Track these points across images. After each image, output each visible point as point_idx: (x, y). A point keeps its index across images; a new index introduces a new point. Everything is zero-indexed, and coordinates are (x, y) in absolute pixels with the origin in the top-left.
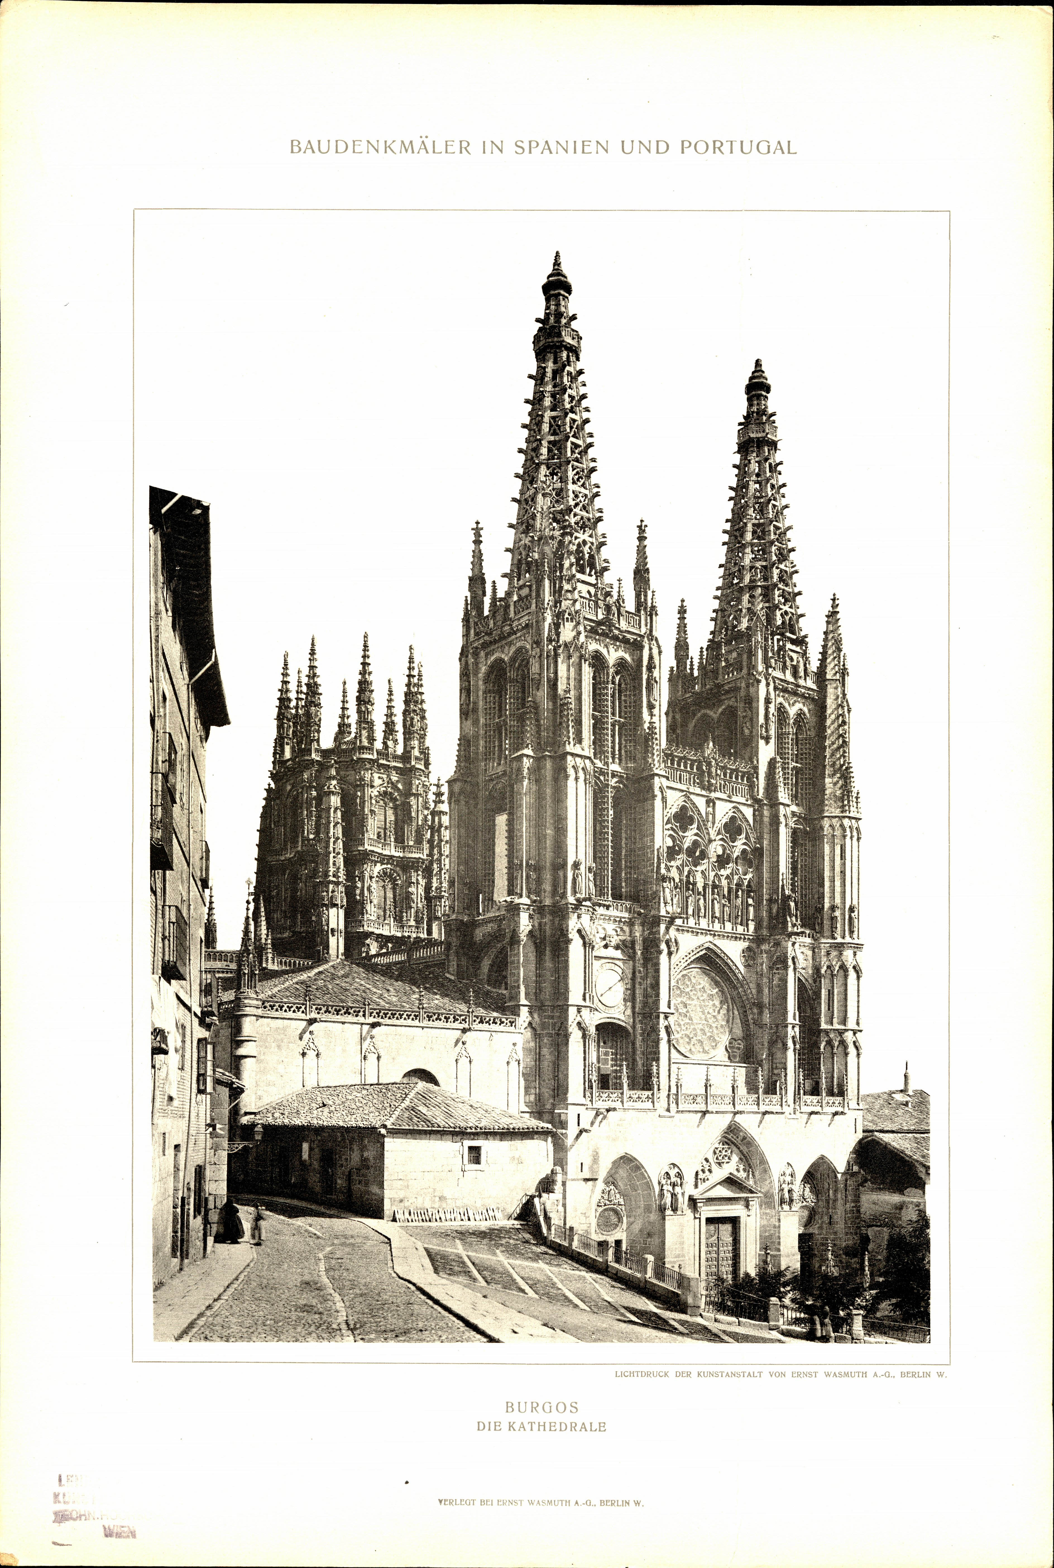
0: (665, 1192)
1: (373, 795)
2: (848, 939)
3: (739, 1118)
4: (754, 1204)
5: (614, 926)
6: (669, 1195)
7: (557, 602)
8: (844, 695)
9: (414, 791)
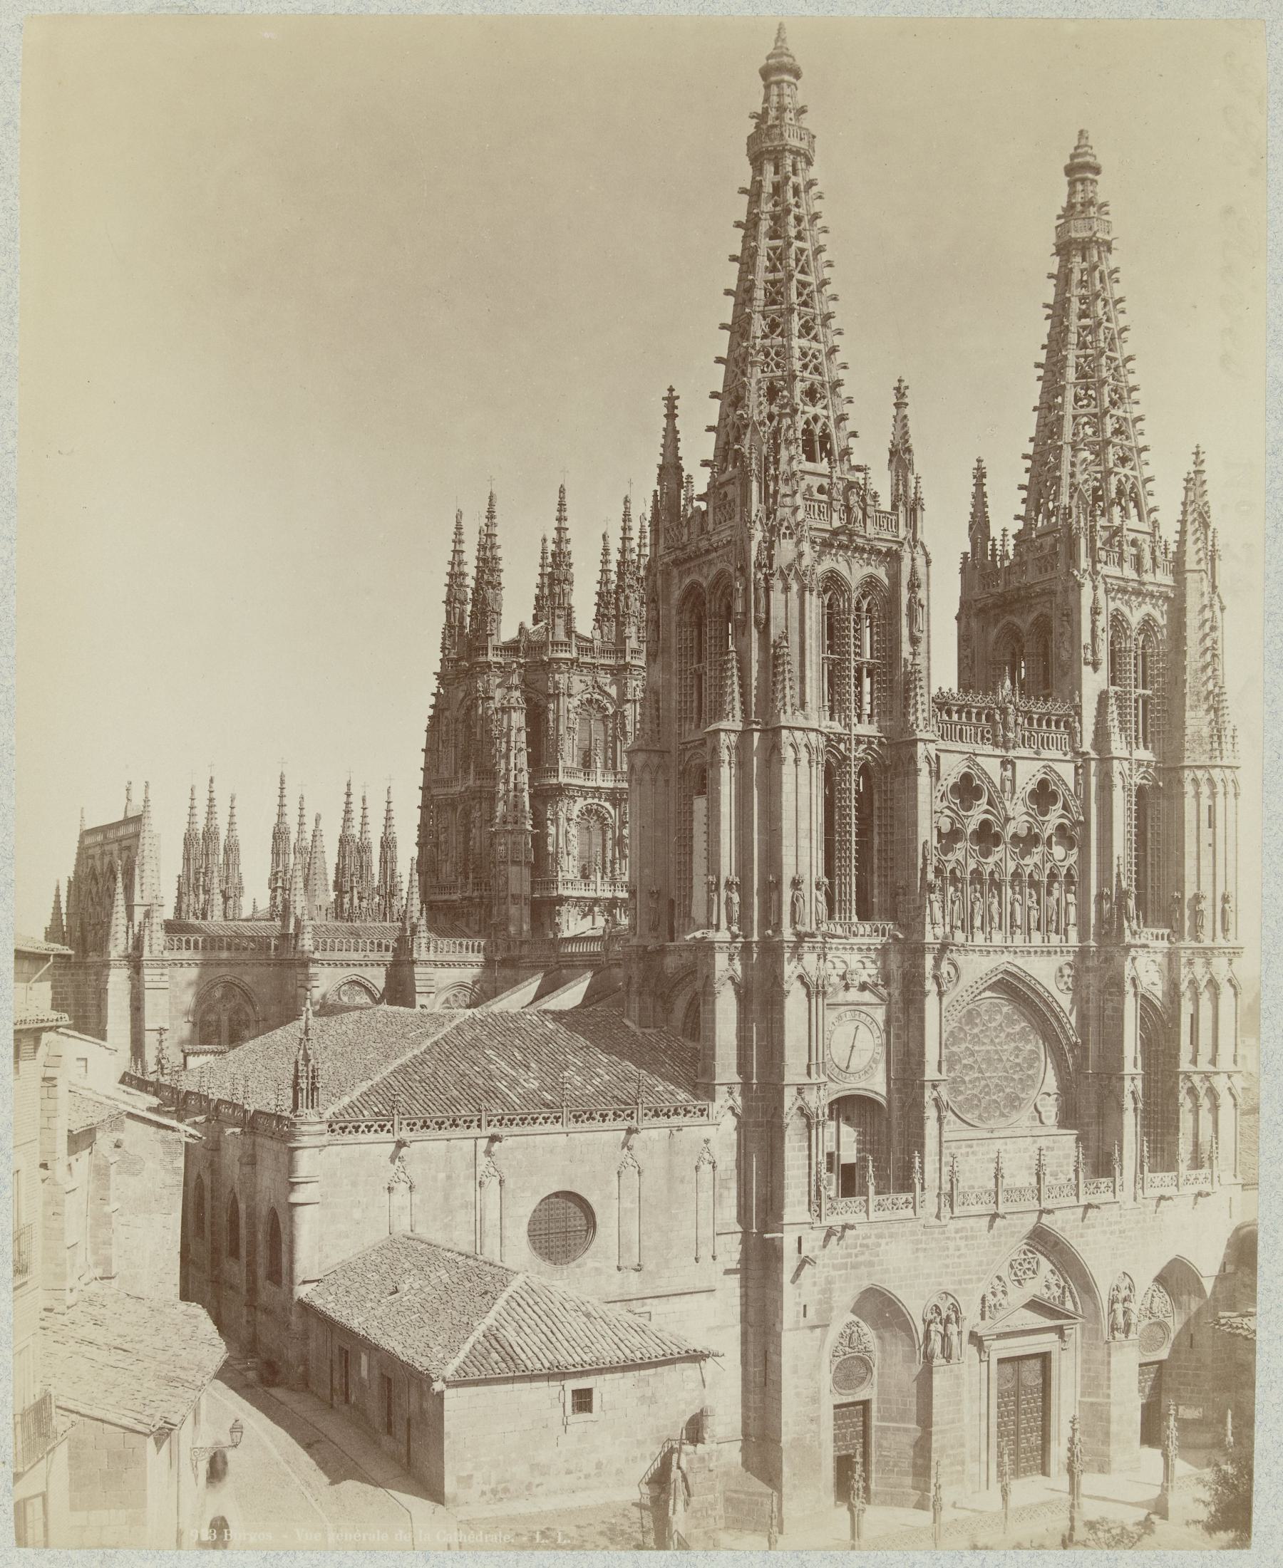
0: (933, 1334)
2: (1220, 941)
3: (1046, 1219)
4: (1075, 1333)
5: (858, 957)
6: (939, 1338)
7: (770, 512)
8: (1214, 587)
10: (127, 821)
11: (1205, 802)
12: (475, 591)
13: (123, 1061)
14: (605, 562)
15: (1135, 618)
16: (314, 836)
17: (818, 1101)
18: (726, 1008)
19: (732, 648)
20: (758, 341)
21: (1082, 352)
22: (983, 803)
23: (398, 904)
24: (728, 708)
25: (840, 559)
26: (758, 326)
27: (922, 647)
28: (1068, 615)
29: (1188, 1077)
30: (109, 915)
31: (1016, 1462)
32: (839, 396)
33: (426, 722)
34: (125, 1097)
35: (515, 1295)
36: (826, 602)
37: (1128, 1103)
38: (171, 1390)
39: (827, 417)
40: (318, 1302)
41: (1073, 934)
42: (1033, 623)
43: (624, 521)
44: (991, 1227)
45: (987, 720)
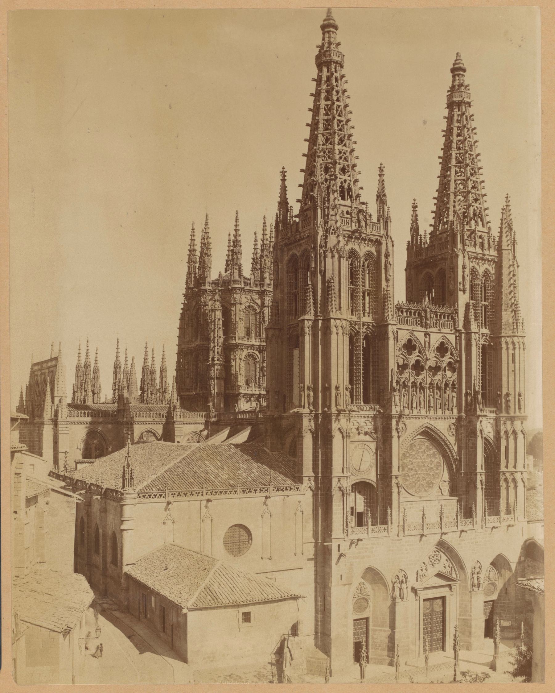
1: (241, 309)
2: (518, 414)
3: (444, 537)
4: (456, 587)
6: (398, 590)
7: (326, 223)
9: (266, 305)
10: (52, 360)
11: (511, 352)
12: (201, 257)
13: (50, 466)
14: (256, 245)
15: (481, 270)
16: (132, 366)
17: (347, 484)
18: (308, 442)
19: (310, 283)
20: (321, 147)
21: (458, 152)
22: (416, 352)
23: (168, 396)
24: (308, 309)
25: (356, 244)
26: (321, 139)
27: (390, 283)
28: (452, 269)
29: (504, 474)
30: (44, 401)
31: (431, 645)
32: (355, 171)
33: (179, 316)
34: (50, 482)
35: (218, 570)
36: (350, 263)
37: (479, 485)
38: (70, 613)
39: (350, 181)
40: (133, 574)
41: (455, 411)
43: (264, 226)
44: (420, 540)
45: (418, 315)
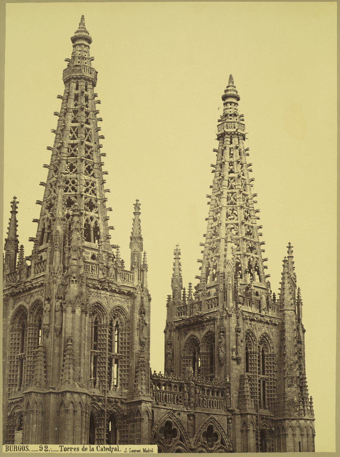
15: (258, 335)
21: (230, 191)
28: (223, 332)
36: (94, 320)
39: (98, 218)
42: (205, 336)
45: (180, 390)
